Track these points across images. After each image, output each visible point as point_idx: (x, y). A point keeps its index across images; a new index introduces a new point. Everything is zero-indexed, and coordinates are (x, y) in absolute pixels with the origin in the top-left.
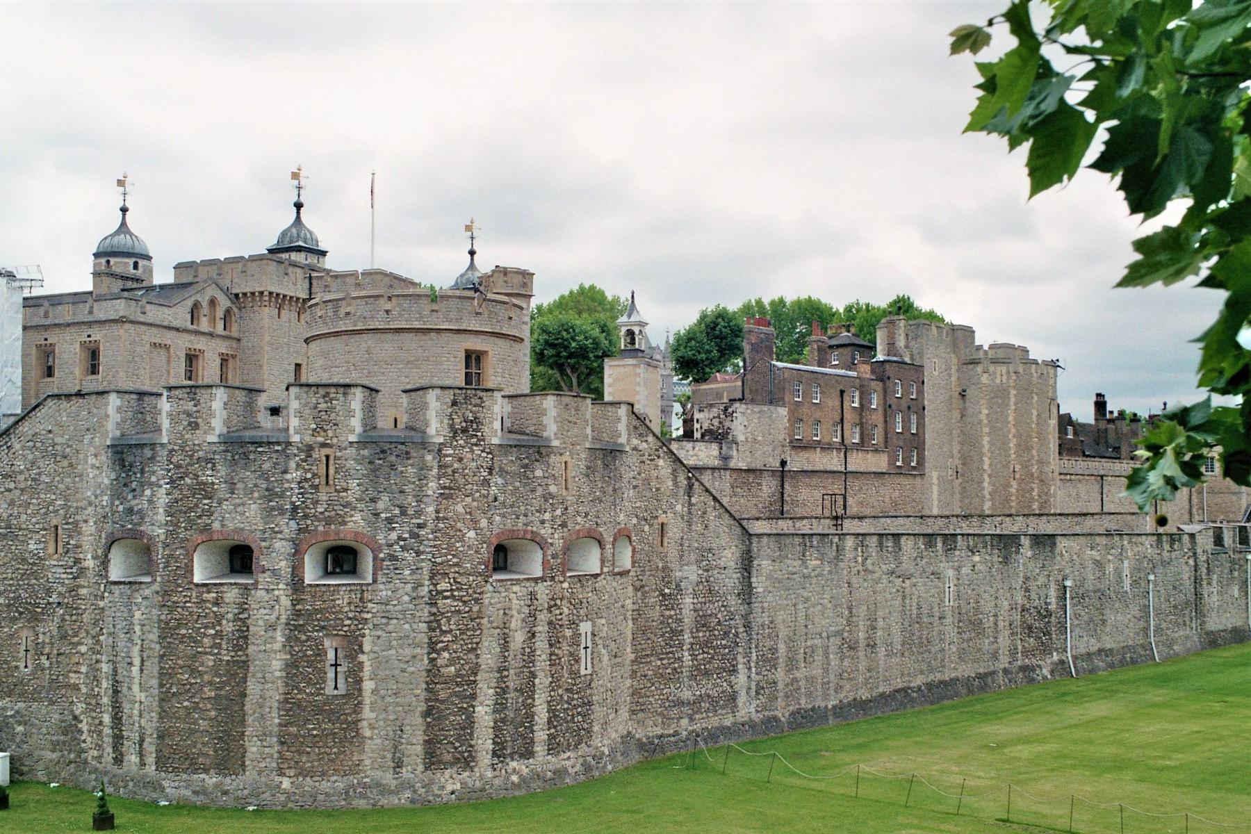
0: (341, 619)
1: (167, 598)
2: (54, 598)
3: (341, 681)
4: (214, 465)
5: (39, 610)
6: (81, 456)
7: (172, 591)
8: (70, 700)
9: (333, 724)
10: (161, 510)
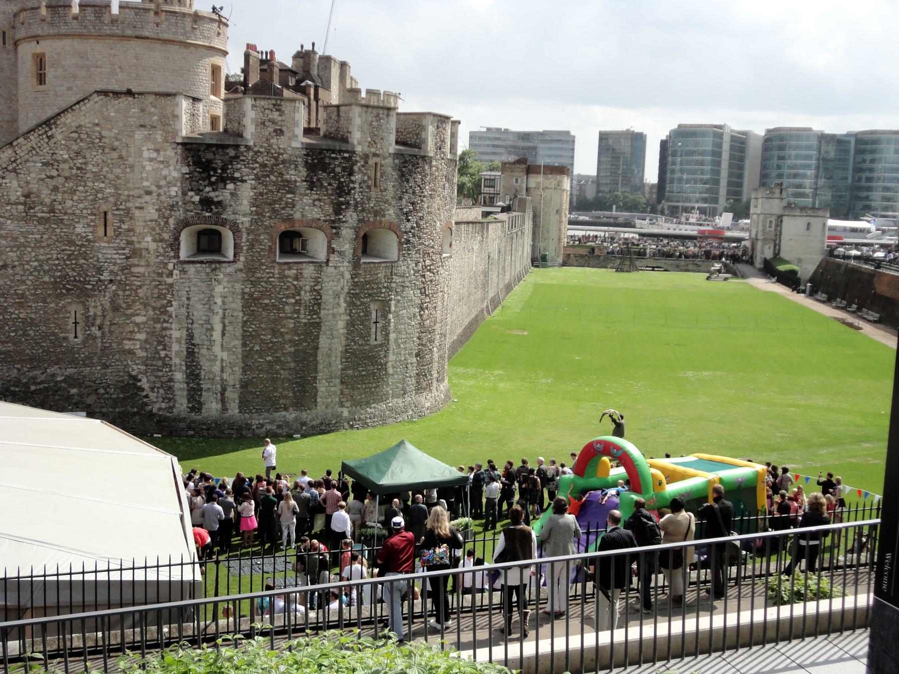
0: (380, 288)
1: (250, 274)
2: (106, 276)
3: (379, 334)
4: (296, 166)
5: (90, 287)
6: (132, 150)
7: (256, 268)
8: (125, 363)
9: (374, 366)
10: (245, 202)
